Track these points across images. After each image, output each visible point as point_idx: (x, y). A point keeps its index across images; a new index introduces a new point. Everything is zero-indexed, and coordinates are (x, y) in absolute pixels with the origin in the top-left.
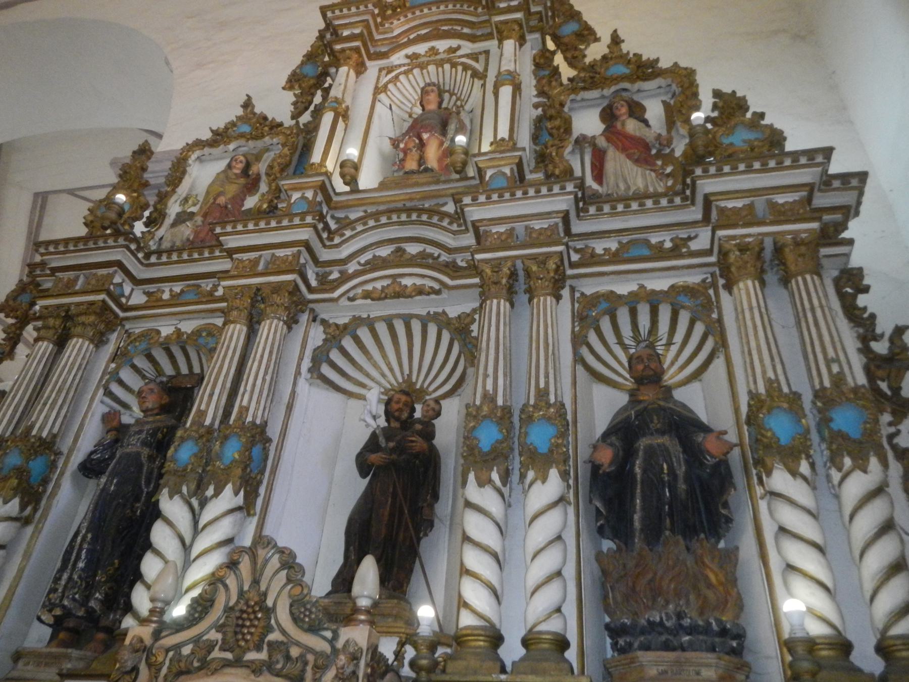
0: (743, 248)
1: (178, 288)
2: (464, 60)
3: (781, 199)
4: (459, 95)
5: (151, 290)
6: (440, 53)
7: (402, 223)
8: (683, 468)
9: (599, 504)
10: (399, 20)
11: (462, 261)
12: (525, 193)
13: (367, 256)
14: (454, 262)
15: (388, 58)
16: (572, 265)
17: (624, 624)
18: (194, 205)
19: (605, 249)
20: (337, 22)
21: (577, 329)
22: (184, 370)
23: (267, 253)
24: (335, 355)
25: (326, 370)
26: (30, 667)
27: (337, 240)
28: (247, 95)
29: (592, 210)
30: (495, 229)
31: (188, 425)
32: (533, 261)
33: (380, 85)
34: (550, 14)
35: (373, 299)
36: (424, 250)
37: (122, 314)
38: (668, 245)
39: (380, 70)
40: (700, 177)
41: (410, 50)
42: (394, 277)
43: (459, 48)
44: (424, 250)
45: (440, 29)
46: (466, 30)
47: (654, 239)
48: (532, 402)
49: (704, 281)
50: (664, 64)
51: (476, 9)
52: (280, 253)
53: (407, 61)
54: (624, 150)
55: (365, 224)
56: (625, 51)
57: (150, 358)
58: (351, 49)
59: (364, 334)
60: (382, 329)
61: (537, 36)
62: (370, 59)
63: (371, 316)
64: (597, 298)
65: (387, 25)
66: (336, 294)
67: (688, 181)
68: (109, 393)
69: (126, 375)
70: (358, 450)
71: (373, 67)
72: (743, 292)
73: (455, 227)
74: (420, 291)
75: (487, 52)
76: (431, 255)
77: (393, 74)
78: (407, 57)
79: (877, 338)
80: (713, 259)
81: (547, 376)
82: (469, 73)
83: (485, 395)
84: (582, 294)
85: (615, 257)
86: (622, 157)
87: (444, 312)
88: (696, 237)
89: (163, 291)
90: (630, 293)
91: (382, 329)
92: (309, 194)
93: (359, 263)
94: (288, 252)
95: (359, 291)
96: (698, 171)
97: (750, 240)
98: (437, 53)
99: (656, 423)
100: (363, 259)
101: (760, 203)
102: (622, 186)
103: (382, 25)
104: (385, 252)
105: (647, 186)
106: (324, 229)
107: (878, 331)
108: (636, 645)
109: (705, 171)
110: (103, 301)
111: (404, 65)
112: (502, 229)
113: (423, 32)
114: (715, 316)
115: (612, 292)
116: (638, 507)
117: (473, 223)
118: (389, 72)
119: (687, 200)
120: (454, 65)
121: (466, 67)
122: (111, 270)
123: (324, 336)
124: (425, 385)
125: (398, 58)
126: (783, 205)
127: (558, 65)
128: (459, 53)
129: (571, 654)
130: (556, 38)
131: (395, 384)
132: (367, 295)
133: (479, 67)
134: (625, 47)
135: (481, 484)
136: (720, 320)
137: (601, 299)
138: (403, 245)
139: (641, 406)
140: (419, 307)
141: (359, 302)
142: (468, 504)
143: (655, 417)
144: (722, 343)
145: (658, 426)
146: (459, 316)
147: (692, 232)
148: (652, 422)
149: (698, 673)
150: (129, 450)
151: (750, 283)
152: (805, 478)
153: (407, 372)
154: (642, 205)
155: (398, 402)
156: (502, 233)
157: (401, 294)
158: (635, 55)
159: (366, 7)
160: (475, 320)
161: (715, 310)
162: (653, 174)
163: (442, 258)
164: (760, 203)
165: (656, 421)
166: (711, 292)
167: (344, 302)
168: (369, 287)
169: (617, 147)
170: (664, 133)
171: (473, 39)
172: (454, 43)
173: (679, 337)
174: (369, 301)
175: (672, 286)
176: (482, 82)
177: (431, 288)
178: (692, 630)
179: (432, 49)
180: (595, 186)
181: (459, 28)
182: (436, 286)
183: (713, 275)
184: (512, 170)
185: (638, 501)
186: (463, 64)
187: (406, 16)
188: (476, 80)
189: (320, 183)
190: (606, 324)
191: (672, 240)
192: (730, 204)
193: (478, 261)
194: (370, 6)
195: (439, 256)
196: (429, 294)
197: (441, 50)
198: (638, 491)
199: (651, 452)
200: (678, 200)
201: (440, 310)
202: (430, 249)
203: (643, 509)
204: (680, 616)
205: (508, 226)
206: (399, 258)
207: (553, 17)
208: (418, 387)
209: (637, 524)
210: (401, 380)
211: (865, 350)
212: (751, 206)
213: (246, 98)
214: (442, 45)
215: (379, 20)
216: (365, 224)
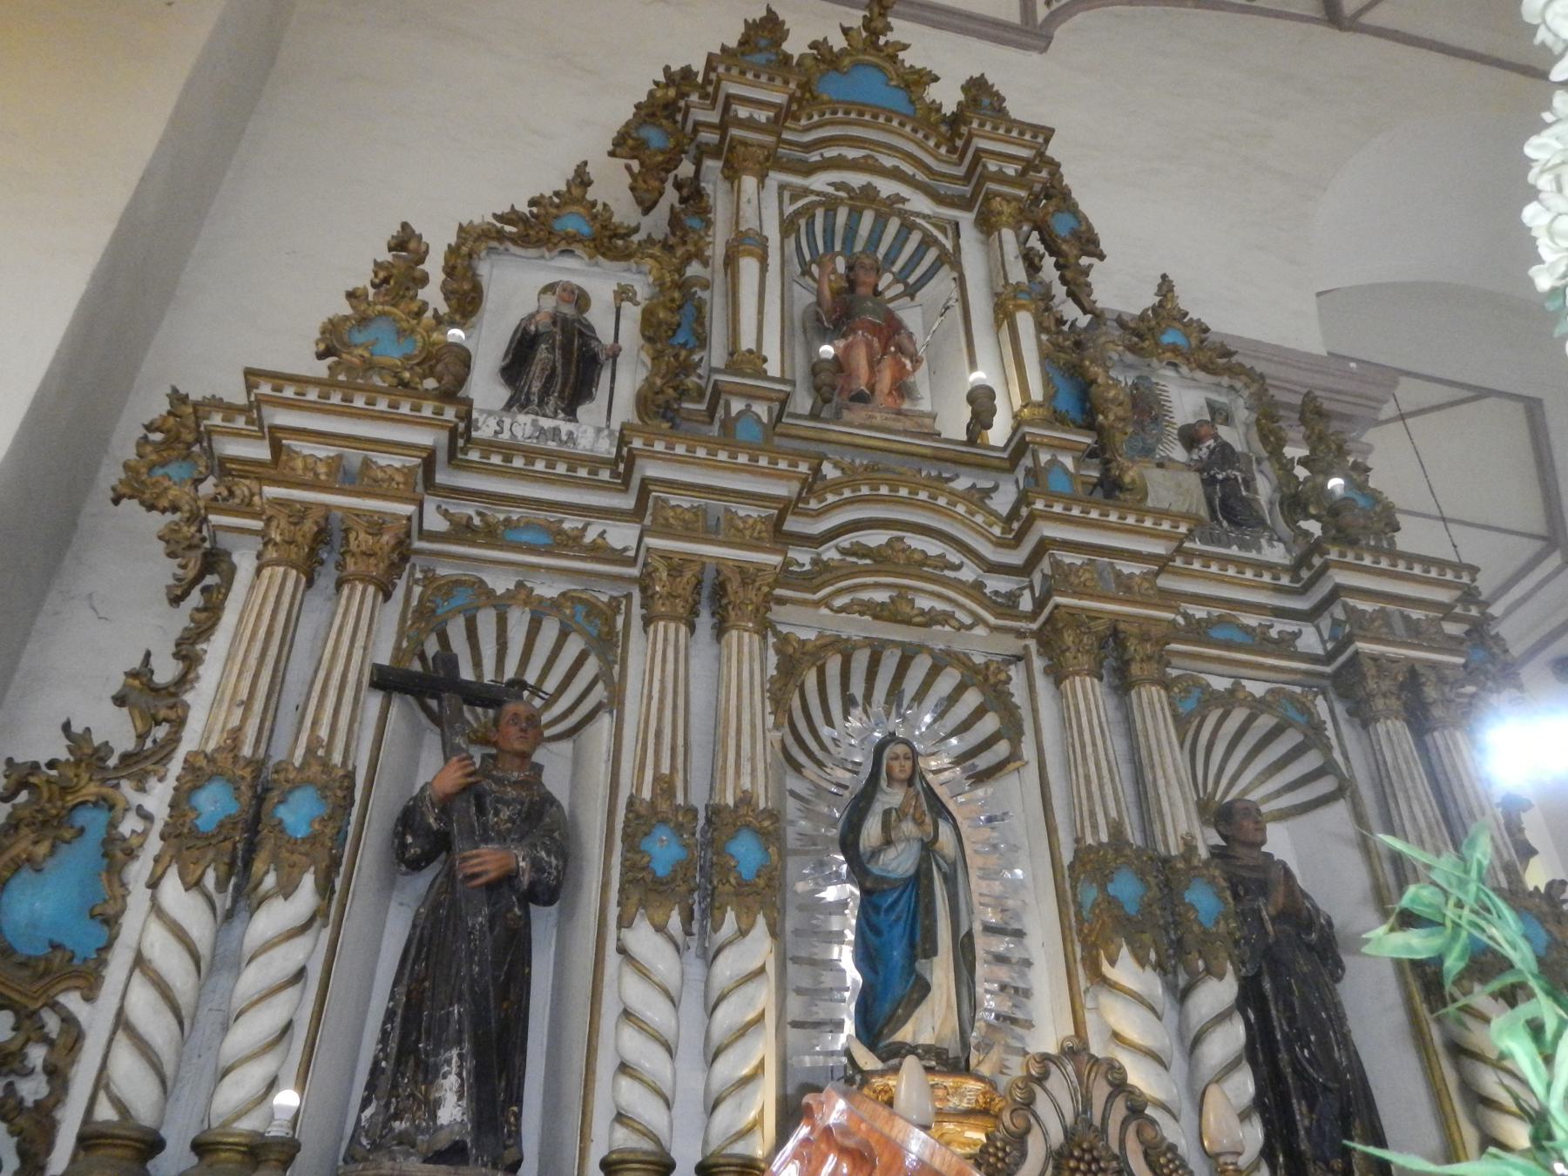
3: (1416, 614)
27: (813, 504)
77: (800, 204)
118: (794, 199)
168: (865, 596)
189: (782, 396)
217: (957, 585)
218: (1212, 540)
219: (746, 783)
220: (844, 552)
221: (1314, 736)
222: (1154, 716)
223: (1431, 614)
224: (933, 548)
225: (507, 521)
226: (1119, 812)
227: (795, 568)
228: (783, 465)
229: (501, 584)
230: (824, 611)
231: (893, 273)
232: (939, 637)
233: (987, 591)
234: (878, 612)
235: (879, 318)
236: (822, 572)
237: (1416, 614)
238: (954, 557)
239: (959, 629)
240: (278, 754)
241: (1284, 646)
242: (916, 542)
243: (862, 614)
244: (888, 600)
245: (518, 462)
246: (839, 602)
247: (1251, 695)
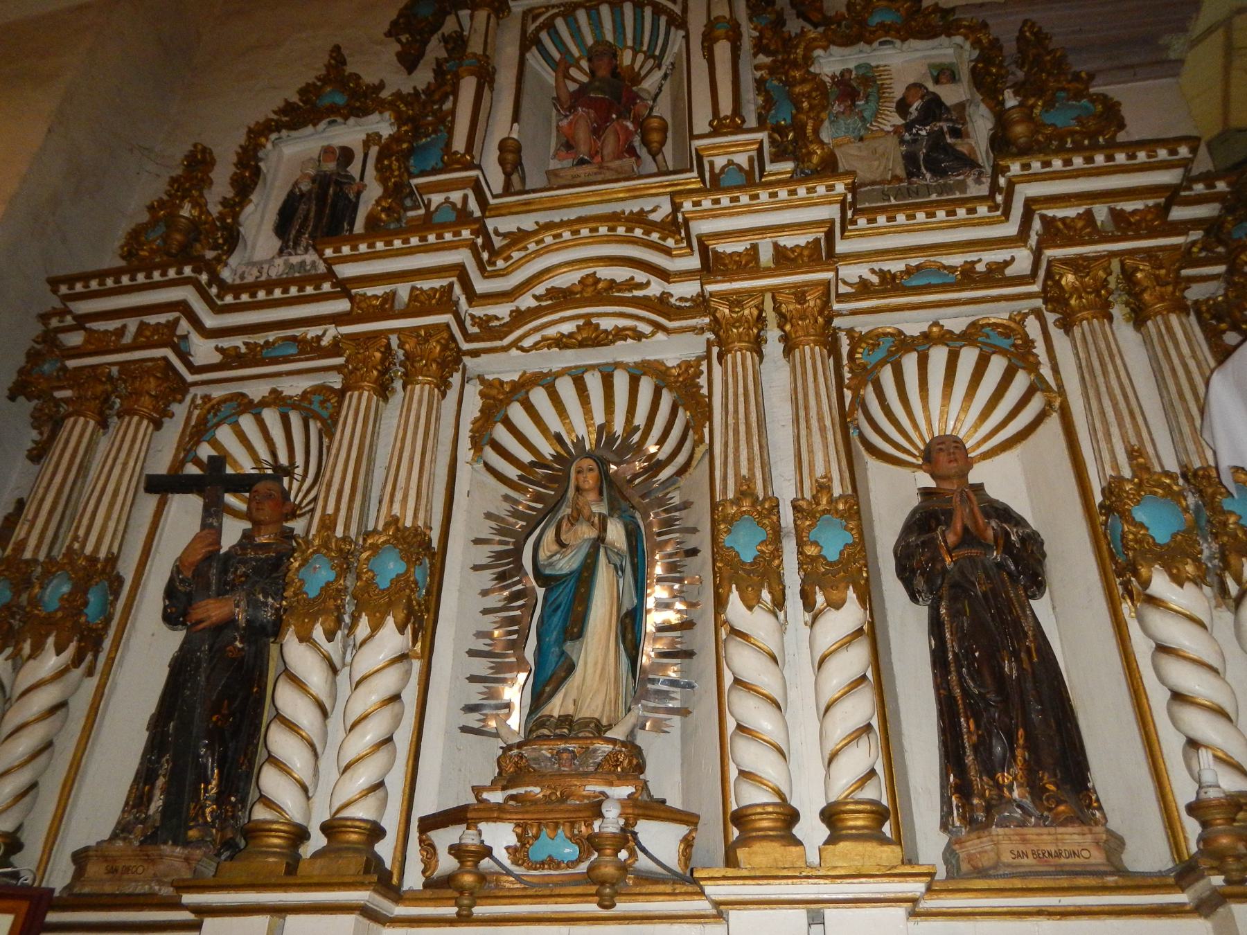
3: (1129, 206)
16: (841, 298)
27: (500, 264)
29: (862, 222)
42: (588, 316)
52: (426, 285)
59: (539, 397)
67: (1002, 181)
73: (670, 242)
80: (1035, 288)
101: (1101, 212)
106: (484, 247)
117: (700, 239)
119: (997, 209)
127: (782, 9)
133: (677, 9)
142: (735, 632)
156: (739, 254)
157: (599, 339)
160: (702, 372)
164: (1101, 212)
168: (552, 332)
176: (682, 33)
193: (711, 294)
206: (604, 293)
217: (644, 303)
218: (909, 193)
219: (396, 510)
220: (536, 297)
221: (1021, 356)
222: (804, 373)
223: (1151, 203)
224: (621, 274)
225: (267, 342)
226: (751, 469)
227: (495, 323)
228: (448, 236)
229: (256, 391)
230: (514, 352)
231: (629, 48)
232: (627, 352)
233: (673, 300)
234: (561, 342)
235: (603, 92)
237: (1129, 206)
238: (640, 276)
239: (639, 340)
241: (995, 275)
242: (605, 273)
243: (549, 347)
244: (575, 330)
245: (261, 295)
246: (527, 343)
247: (951, 332)
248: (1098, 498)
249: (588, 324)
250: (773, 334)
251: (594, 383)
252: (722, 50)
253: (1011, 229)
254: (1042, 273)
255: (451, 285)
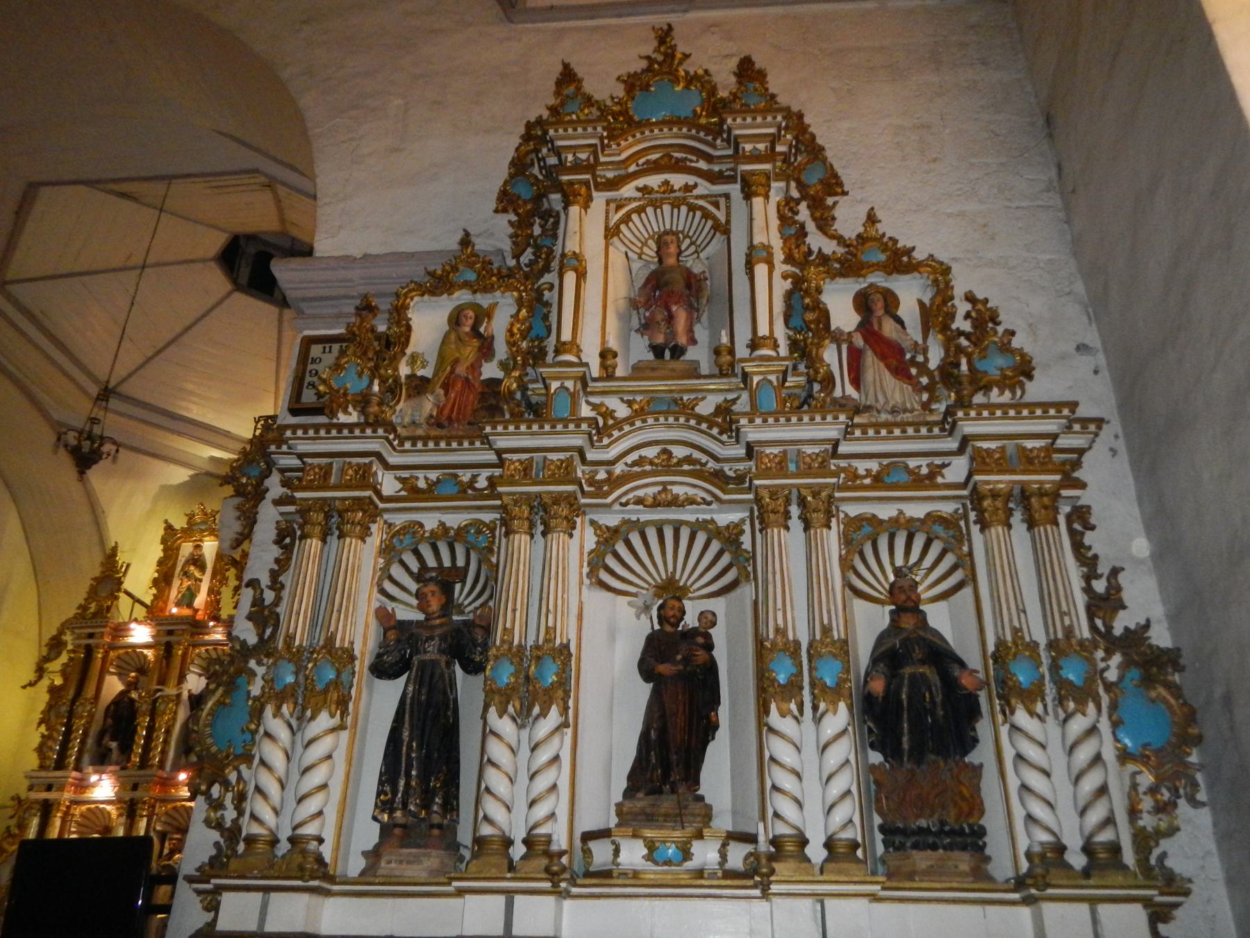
0: (995, 495)
1: (433, 475)
2: (701, 203)
3: (1029, 444)
4: (694, 239)
5: (403, 476)
6: (675, 191)
7: (670, 426)
8: (940, 696)
9: (872, 725)
10: (626, 140)
11: (730, 469)
12: (800, 419)
13: (634, 456)
14: (722, 470)
15: (617, 190)
17: (898, 828)
18: (424, 367)
19: (866, 470)
20: (560, 143)
21: (843, 552)
22: (447, 563)
23: (537, 456)
24: (611, 562)
25: (604, 576)
26: (393, 865)
27: (606, 441)
28: (465, 230)
30: (768, 451)
31: (498, 643)
32: (809, 491)
33: (612, 224)
34: (793, 151)
35: (645, 506)
36: (691, 455)
37: (381, 505)
38: (924, 471)
39: (608, 203)
40: (961, 420)
41: (641, 182)
42: (664, 484)
43: (696, 186)
44: (691, 455)
45: (672, 156)
46: (702, 165)
47: (912, 463)
48: (818, 637)
49: (956, 511)
50: (919, 255)
51: (714, 139)
53: (639, 195)
54: (883, 357)
55: (632, 424)
56: (881, 232)
57: (416, 552)
58: (580, 182)
60: (652, 534)
61: (782, 184)
62: (597, 189)
63: (641, 520)
64: (860, 520)
65: (614, 147)
66: (609, 500)
68: (383, 592)
69: (397, 571)
70: (638, 656)
71: (600, 198)
72: (994, 536)
73: (724, 437)
74: (692, 501)
75: (727, 196)
76: (697, 462)
78: (638, 189)
79: (1098, 577)
80: (965, 493)
81: (829, 612)
82: (710, 223)
83: (777, 630)
84: (846, 515)
85: (878, 480)
86: (882, 365)
87: (713, 521)
88: (949, 464)
89: (417, 478)
90: (890, 519)
91: (652, 534)
92: (569, 384)
93: (626, 464)
94: (562, 456)
95: (631, 496)
96: (960, 414)
97: (1002, 486)
98: (673, 191)
99: (918, 654)
100: (630, 459)
102: (881, 400)
103: (609, 146)
104: (651, 452)
105: (904, 402)
107: (1099, 571)
108: (908, 844)
109: (967, 414)
110: (370, 498)
111: (635, 199)
112: (776, 450)
113: (654, 157)
114: (965, 549)
115: (874, 516)
116: (906, 731)
118: (618, 208)
120: (692, 208)
121: (706, 215)
122: (367, 460)
123: (596, 539)
124: (689, 584)
125: (628, 190)
126: (1031, 450)
128: (696, 192)
129: (859, 853)
130: (801, 186)
131: (659, 581)
132: (639, 501)
133: (721, 216)
134: (881, 228)
135: (783, 715)
136: (970, 554)
137: (864, 523)
138: (669, 447)
139: (904, 635)
140: (688, 515)
141: (630, 507)
143: (917, 648)
144: (973, 578)
145: (920, 656)
146: (728, 527)
147: (946, 460)
148: (914, 651)
149: (956, 867)
150: (427, 657)
151: (1000, 529)
152: (1039, 717)
153: (670, 569)
154: (904, 431)
155: (672, 608)
156: (776, 456)
157: (675, 502)
158: (890, 238)
159: (595, 128)
161: (966, 543)
162: (910, 387)
163: (710, 465)
165: (917, 651)
166: (962, 523)
167: (617, 507)
168: (640, 493)
169: (875, 353)
170: (920, 341)
171: (713, 178)
172: (691, 179)
173: (927, 562)
174: (641, 507)
175: (929, 515)
177: (703, 499)
178: (952, 833)
179: (666, 183)
180: (850, 391)
181: (694, 158)
182: (709, 498)
183: (964, 505)
184: (778, 378)
185: (905, 725)
186: (701, 208)
187: (634, 136)
188: (718, 234)
190: (868, 550)
191: (928, 465)
192: (985, 445)
194: (599, 129)
195: (707, 463)
196: (699, 504)
197: (676, 187)
198: (905, 716)
199: (913, 677)
200: (936, 430)
201: (708, 517)
202: (697, 455)
203: (910, 732)
204: (943, 823)
205: (781, 449)
207: (795, 155)
208: (681, 584)
209: (906, 746)
210: (664, 577)
211: (1088, 590)
212: (1003, 448)
213: (463, 233)
214: (678, 180)
215: (606, 141)
216: (632, 424)
236: (614, 482)
237: (1029, 444)
240: (304, 644)
248: (991, 648)
249: (665, 490)
250: (795, 510)
251: (669, 533)
252: (761, 270)
253: (953, 444)
254: (970, 486)
255: (572, 456)
